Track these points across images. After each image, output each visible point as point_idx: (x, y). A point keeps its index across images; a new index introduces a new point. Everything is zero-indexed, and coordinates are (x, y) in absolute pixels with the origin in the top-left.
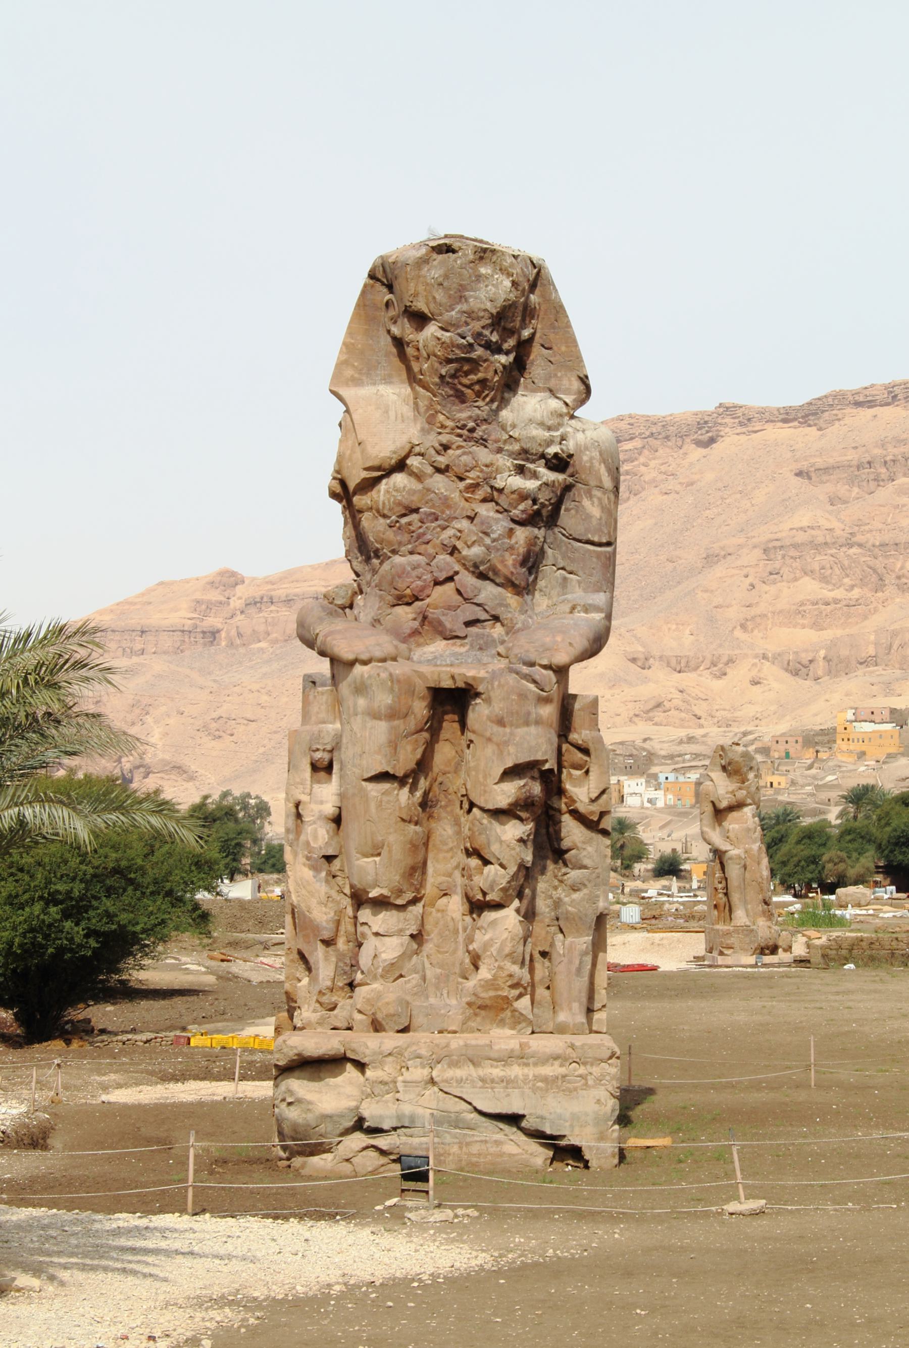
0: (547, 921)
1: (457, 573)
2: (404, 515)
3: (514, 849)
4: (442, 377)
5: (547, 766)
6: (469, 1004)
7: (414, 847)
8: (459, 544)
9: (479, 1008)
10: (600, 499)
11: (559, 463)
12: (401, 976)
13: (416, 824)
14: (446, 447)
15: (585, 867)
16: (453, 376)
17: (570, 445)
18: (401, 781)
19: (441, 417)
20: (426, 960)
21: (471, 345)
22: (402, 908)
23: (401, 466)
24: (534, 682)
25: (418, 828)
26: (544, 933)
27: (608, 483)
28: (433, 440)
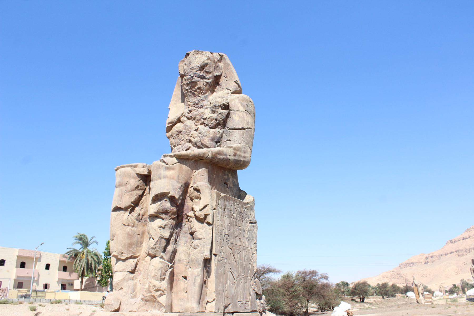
0: (185, 263)
1: (190, 147)
2: (178, 134)
3: (157, 231)
4: (187, 90)
5: (170, 195)
6: (142, 299)
7: (130, 236)
8: (192, 139)
9: (146, 301)
10: (239, 115)
11: (226, 107)
12: (122, 288)
13: (133, 226)
14: (190, 111)
15: (199, 239)
16: (190, 89)
17: (228, 101)
18: (125, 209)
19: (189, 103)
20: (138, 282)
21: (192, 77)
22: (124, 260)
23: (179, 121)
24: (164, 162)
25: (133, 228)
26: (184, 268)
27: (242, 109)
28: (187, 110)
